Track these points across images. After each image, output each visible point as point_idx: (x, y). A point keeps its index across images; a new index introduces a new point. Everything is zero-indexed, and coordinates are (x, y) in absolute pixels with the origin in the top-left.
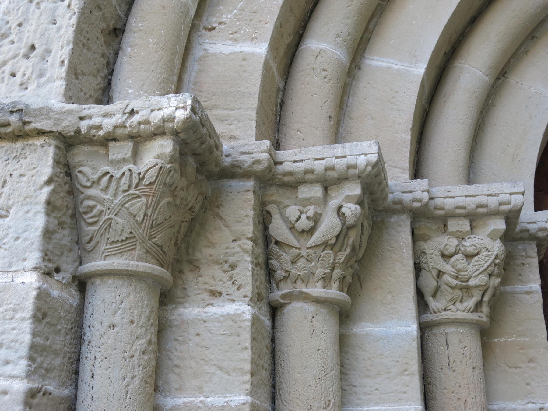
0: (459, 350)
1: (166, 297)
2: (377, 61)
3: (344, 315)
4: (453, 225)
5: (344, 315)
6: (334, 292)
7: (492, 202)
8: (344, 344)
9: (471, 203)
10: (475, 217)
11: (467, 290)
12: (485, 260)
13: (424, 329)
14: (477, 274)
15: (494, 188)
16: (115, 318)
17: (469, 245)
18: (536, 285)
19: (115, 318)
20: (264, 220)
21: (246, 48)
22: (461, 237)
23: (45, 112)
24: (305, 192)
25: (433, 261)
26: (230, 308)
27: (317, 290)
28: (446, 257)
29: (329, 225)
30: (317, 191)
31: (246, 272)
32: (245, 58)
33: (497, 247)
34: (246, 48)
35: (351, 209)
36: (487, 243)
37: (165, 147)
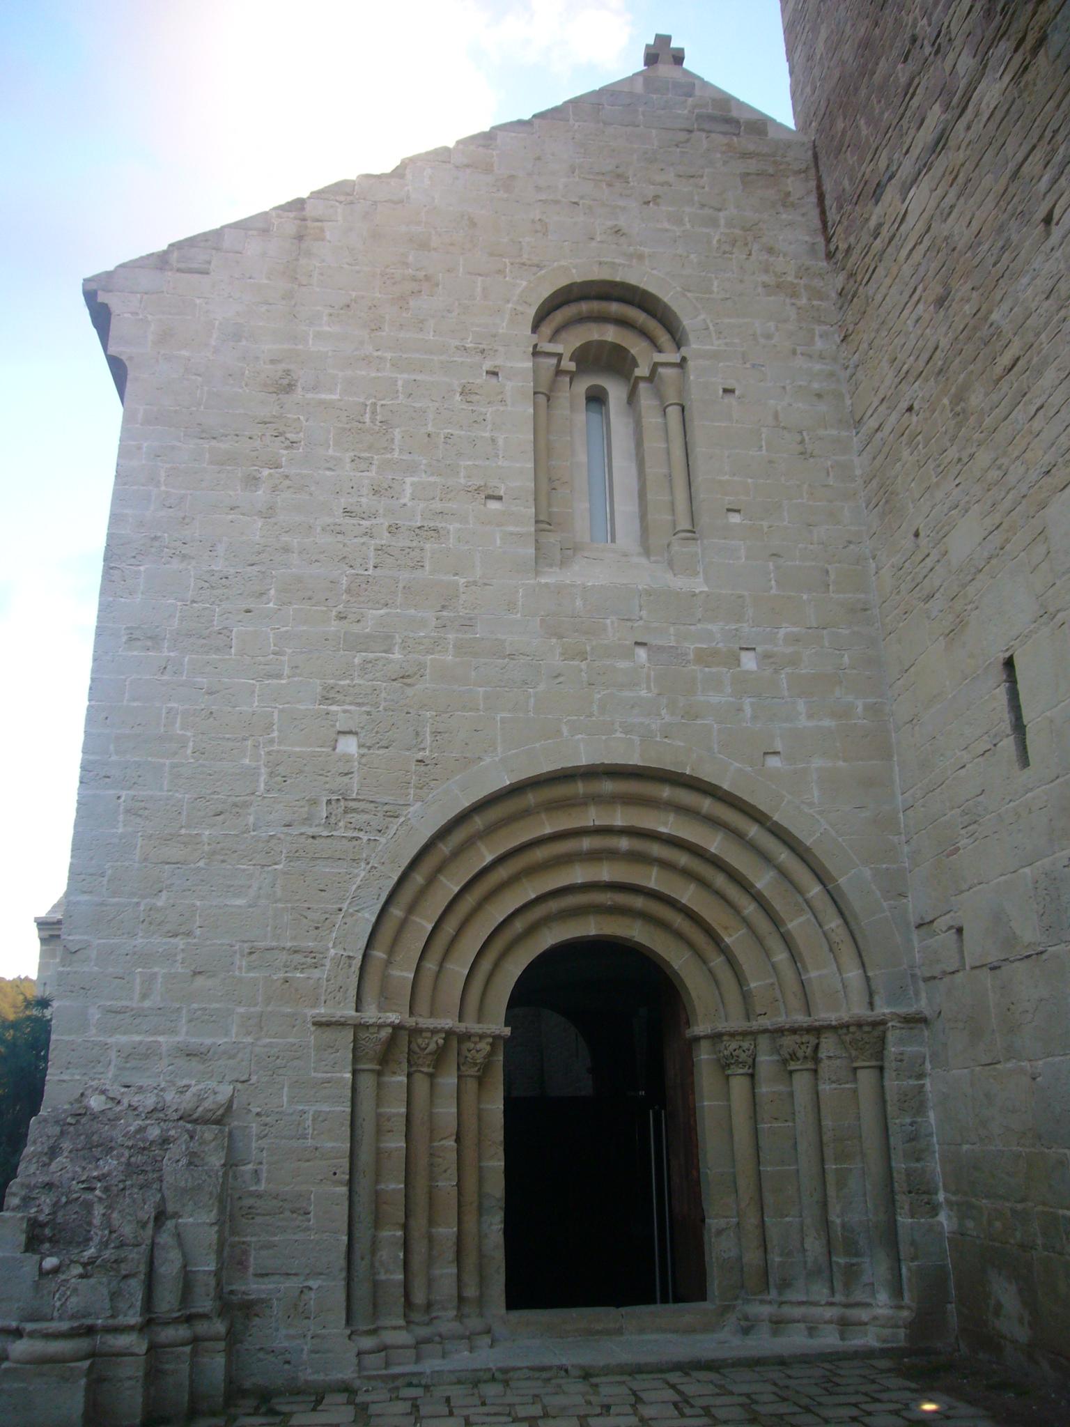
0: (471, 1085)
1: (379, 1074)
2: (449, 966)
3: (432, 1076)
4: (473, 1039)
5: (432, 1076)
6: (431, 1070)
7: (488, 1032)
8: (432, 1086)
9: (480, 1031)
10: (482, 1037)
11: (475, 1064)
12: (483, 1053)
13: (459, 1077)
14: (480, 1058)
15: (491, 1026)
16: (367, 1082)
17: (479, 1046)
18: (501, 1058)
19: (367, 1082)
20: (410, 1042)
21: (405, 974)
22: (476, 1043)
23: (352, 1017)
24: (424, 1034)
25: (465, 1053)
26: (400, 1078)
27: (425, 1070)
28: (469, 1051)
29: (432, 1047)
30: (429, 1034)
31: (405, 1065)
32: (405, 978)
33: (488, 1048)
34: (405, 974)
35: (441, 1042)
36: (484, 1046)
37: (390, 1030)
